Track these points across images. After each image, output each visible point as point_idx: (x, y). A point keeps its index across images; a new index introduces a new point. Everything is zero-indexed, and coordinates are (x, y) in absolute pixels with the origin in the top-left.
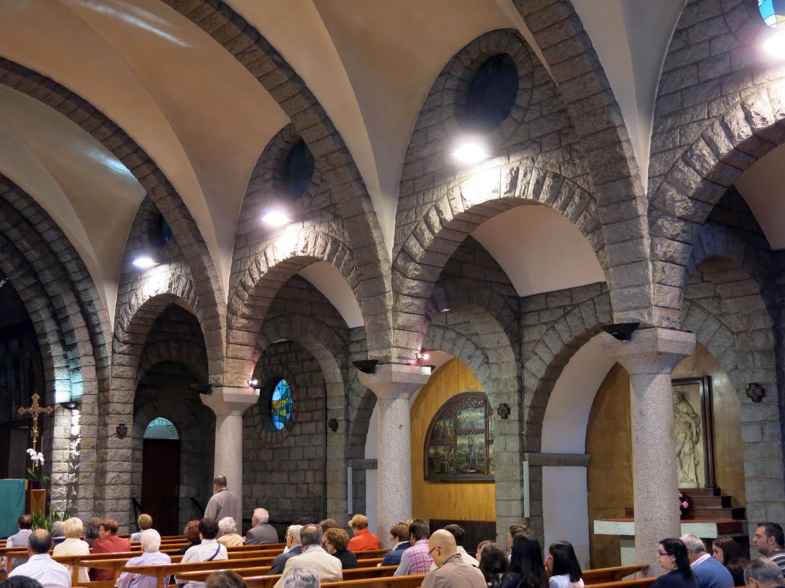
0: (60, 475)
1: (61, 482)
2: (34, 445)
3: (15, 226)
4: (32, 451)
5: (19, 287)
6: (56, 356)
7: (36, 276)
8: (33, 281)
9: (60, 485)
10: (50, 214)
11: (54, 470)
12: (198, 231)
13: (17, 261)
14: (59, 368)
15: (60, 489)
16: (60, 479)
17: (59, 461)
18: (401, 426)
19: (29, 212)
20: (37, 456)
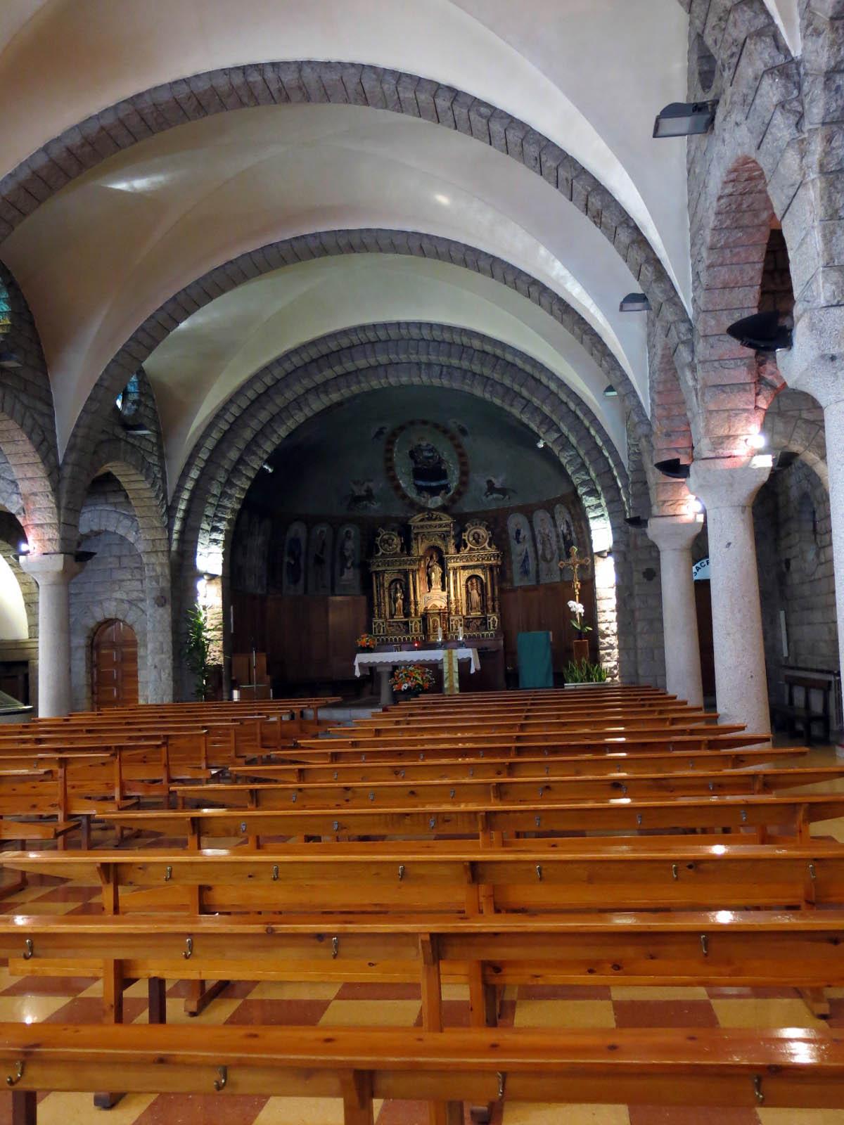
0: (607, 625)
1: (609, 632)
2: (577, 597)
3: (521, 386)
4: (572, 604)
5: (550, 444)
6: (589, 507)
7: (559, 430)
8: (556, 435)
9: (608, 636)
10: (546, 366)
11: (599, 620)
12: (604, 345)
13: (538, 419)
14: (594, 518)
15: (607, 639)
16: (607, 628)
17: (604, 611)
18: (729, 544)
19: (528, 368)
20: (577, 607)
